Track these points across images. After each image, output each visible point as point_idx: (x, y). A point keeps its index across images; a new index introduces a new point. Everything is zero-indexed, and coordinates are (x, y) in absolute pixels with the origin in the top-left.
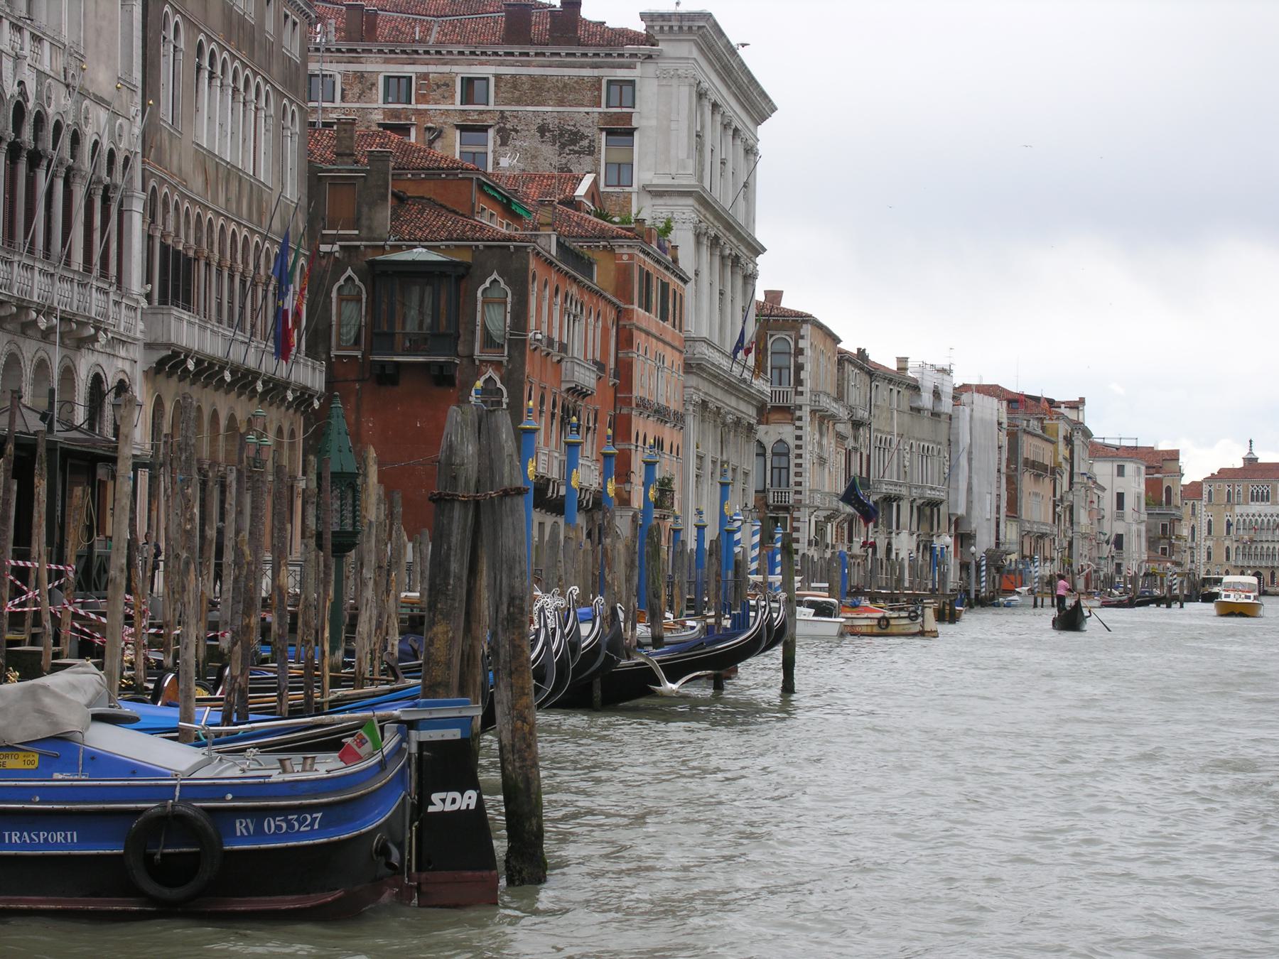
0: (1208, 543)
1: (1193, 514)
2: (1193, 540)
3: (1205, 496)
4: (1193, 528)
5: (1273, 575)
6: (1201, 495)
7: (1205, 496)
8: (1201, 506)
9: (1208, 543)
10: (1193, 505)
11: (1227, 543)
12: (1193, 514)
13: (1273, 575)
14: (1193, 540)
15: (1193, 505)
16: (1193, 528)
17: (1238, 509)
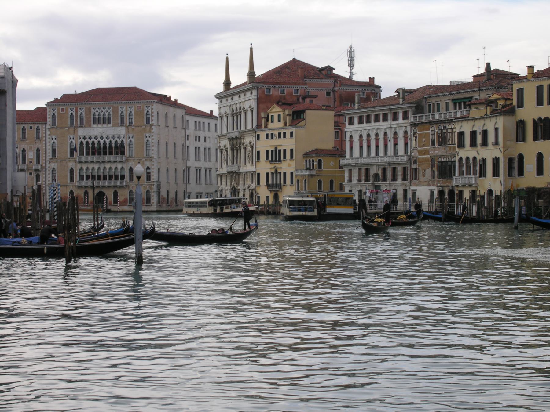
0: (53, 165)
1: (38, 138)
2: (38, 162)
3: (49, 120)
4: (38, 150)
5: (116, 194)
6: (45, 119)
7: (49, 120)
8: (46, 130)
9: (53, 165)
10: (38, 129)
11: (71, 165)
12: (38, 138)
13: (116, 194)
14: (38, 162)
15: (38, 129)
16: (38, 150)
17: (81, 132)
